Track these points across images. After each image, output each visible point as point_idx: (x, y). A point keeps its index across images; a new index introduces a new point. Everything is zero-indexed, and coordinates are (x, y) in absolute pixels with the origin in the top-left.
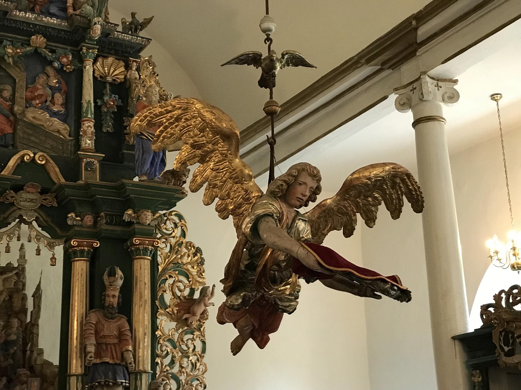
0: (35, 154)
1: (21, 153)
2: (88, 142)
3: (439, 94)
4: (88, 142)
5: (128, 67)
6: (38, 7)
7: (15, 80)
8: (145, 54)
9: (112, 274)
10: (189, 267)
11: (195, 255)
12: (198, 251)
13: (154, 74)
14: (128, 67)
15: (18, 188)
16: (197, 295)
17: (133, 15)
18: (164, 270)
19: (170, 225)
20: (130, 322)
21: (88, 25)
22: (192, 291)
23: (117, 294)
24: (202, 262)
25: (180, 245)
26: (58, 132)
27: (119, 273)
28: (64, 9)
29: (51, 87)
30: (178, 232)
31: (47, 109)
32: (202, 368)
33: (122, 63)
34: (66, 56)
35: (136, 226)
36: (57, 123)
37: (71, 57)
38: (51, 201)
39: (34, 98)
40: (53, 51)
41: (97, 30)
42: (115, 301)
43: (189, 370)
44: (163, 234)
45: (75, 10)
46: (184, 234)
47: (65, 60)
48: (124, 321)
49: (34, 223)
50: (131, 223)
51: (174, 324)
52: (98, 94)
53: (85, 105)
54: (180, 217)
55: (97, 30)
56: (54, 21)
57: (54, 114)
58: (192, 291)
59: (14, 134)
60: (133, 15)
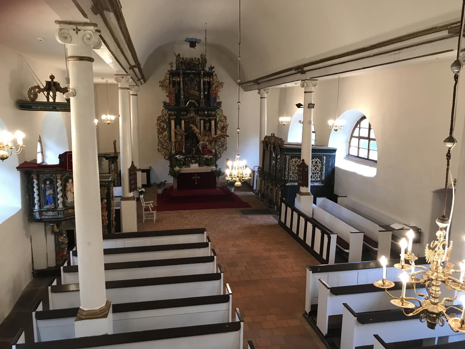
0: (192, 100)
1: (190, 101)
2: (202, 97)
3: (265, 92)
4: (202, 97)
5: (210, 78)
6: (191, 68)
7: (188, 84)
8: (214, 74)
9: (207, 124)
10: (223, 120)
11: (225, 118)
12: (225, 117)
13: (217, 77)
14: (210, 78)
15: (189, 108)
16: (225, 126)
17: (211, 66)
18: (218, 121)
19: (219, 112)
20: (211, 132)
21: (201, 72)
22: (224, 125)
23: (208, 128)
24: (226, 119)
25: (221, 116)
26: (197, 94)
27: (208, 124)
28: (196, 68)
29: (195, 84)
30: (221, 113)
31: (194, 89)
32: (226, 140)
33: (209, 77)
34: (197, 78)
35: (211, 115)
36: (196, 92)
37: (198, 78)
38: (195, 109)
39: (192, 87)
40: (195, 77)
41: (202, 73)
42: (208, 129)
43: (223, 140)
44: (218, 114)
45: (198, 68)
46: (222, 114)
47: (197, 79)
48: (209, 133)
49: (194, 113)
50: (210, 114)
51: (220, 132)
52: (204, 85)
53: (201, 88)
54: (222, 110)
55: (202, 73)
56: (194, 71)
57: (196, 90)
58: (224, 125)
59: (188, 96)
60: (211, 66)
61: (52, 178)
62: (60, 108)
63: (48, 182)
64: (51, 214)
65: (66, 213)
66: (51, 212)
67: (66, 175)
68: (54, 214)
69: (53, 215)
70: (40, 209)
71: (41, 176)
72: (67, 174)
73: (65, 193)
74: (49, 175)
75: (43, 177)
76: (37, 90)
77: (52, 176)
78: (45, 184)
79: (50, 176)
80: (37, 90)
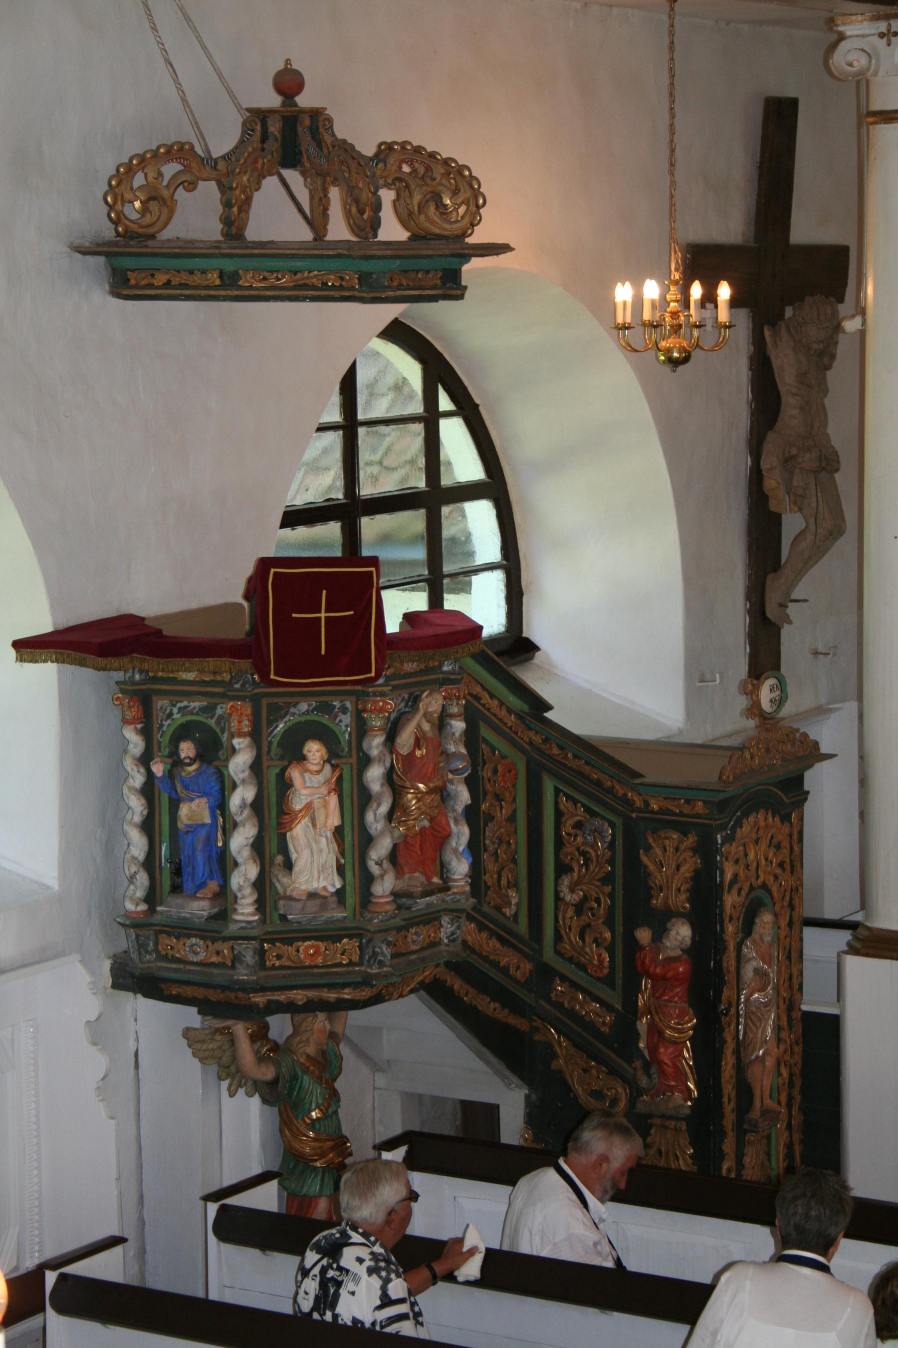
61: (212, 722)
62: (265, 279)
63: (187, 749)
64: (201, 956)
65: (285, 962)
66: (201, 943)
67: (292, 710)
68: (214, 959)
69: (213, 965)
70: (152, 910)
71: (161, 703)
72: (304, 707)
73: (283, 831)
74: (196, 705)
75: (170, 715)
76: (170, 169)
77: (209, 710)
78: (177, 762)
79: (203, 710)
80: (170, 169)
